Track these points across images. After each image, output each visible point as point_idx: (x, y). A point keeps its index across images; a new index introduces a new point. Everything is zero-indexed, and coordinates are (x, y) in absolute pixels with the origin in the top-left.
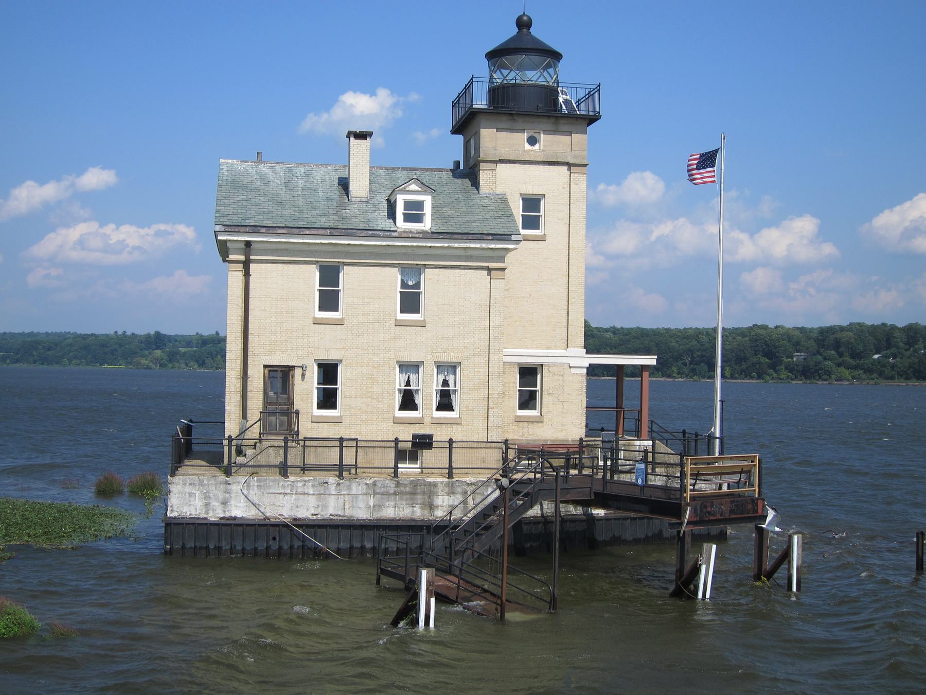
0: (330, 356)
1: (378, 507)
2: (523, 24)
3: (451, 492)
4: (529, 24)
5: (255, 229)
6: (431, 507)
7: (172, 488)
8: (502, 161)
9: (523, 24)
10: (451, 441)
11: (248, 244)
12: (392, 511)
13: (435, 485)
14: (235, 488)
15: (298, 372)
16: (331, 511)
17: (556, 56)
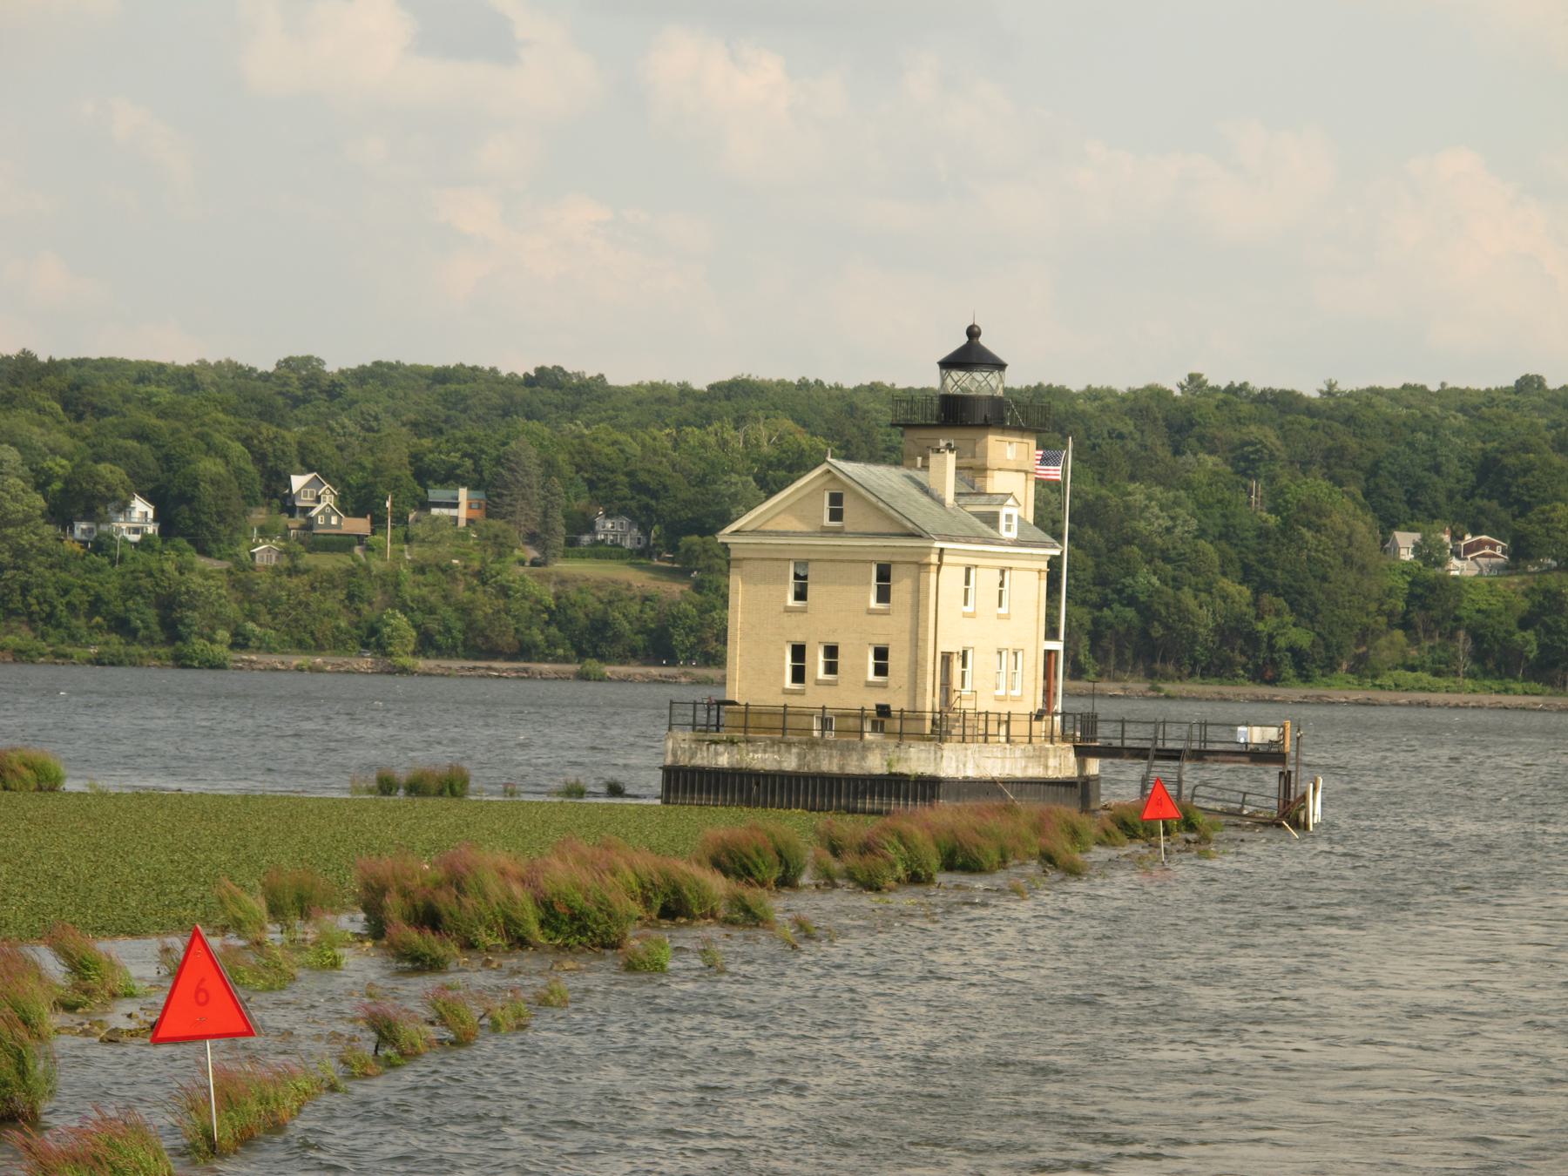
0: (967, 644)
1: (1026, 767)
2: (973, 333)
3: (1055, 756)
4: (979, 334)
5: (951, 539)
6: (1046, 767)
7: (945, 753)
8: (1000, 469)
9: (973, 333)
10: (1009, 714)
11: (942, 550)
12: (1034, 771)
13: (1047, 749)
14: (969, 752)
15: (955, 656)
16: (1007, 771)
17: (1000, 366)
